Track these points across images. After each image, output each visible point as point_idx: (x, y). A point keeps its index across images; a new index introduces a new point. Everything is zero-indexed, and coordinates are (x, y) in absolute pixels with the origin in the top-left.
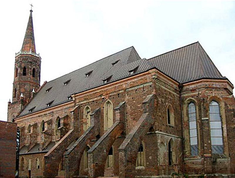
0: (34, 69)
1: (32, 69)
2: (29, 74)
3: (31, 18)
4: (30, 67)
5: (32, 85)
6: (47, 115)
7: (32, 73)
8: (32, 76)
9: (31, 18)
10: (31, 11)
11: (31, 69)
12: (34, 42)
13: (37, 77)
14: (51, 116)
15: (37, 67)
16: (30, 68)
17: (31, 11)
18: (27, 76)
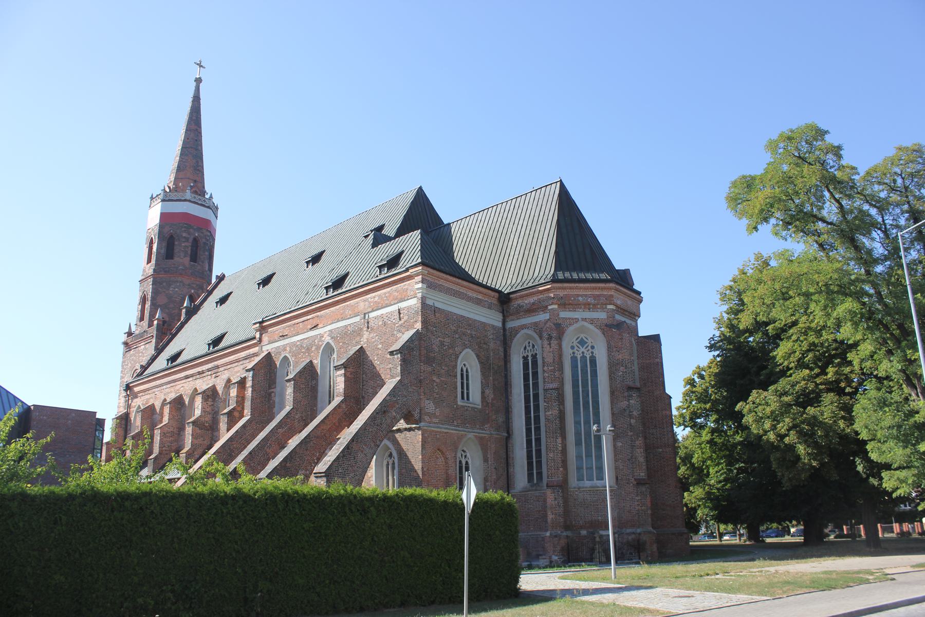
0: (196, 240)
1: (191, 240)
2: (182, 254)
3: (196, 99)
4: (184, 235)
5: (189, 285)
6: (205, 375)
7: (189, 252)
8: (188, 259)
9: (196, 99)
10: (198, 81)
11: (187, 239)
12: (200, 164)
13: (203, 262)
14: (214, 375)
15: (202, 233)
16: (185, 237)
17: (198, 81)
18: (176, 259)
